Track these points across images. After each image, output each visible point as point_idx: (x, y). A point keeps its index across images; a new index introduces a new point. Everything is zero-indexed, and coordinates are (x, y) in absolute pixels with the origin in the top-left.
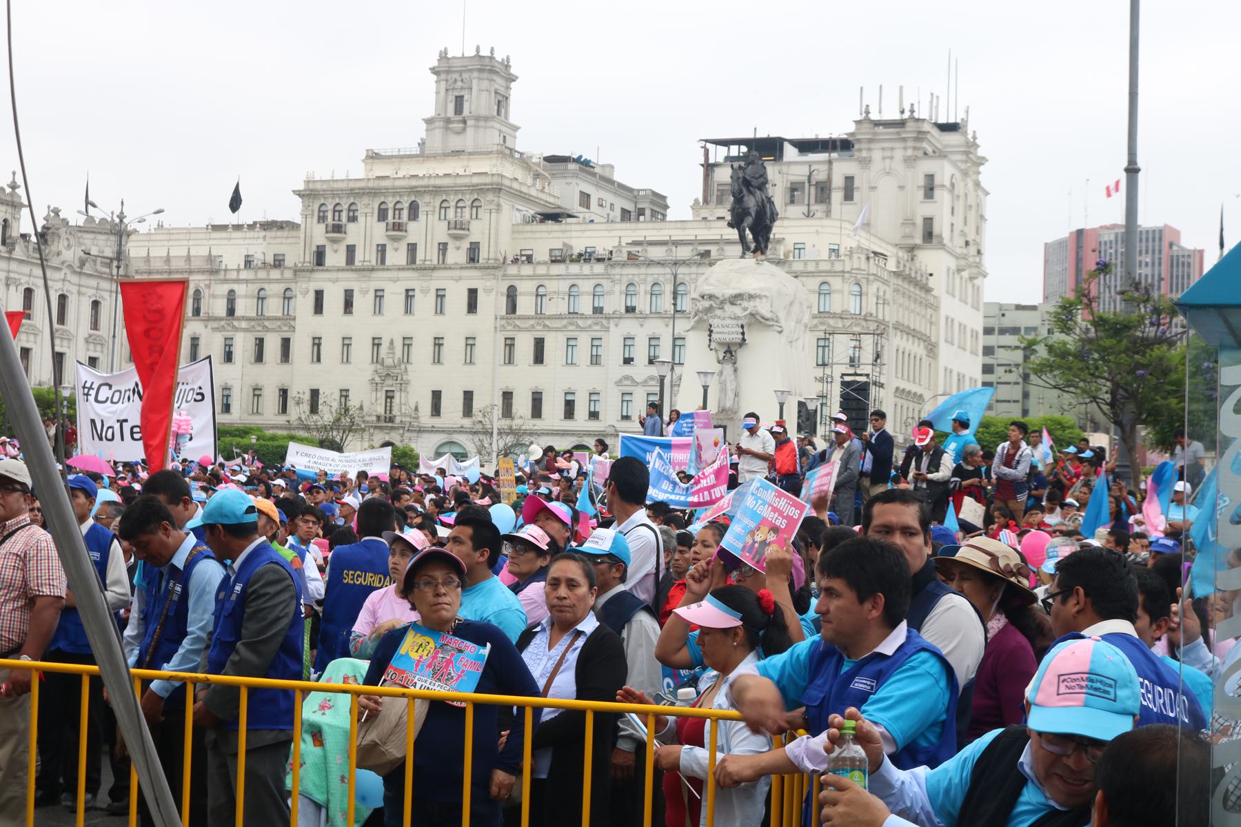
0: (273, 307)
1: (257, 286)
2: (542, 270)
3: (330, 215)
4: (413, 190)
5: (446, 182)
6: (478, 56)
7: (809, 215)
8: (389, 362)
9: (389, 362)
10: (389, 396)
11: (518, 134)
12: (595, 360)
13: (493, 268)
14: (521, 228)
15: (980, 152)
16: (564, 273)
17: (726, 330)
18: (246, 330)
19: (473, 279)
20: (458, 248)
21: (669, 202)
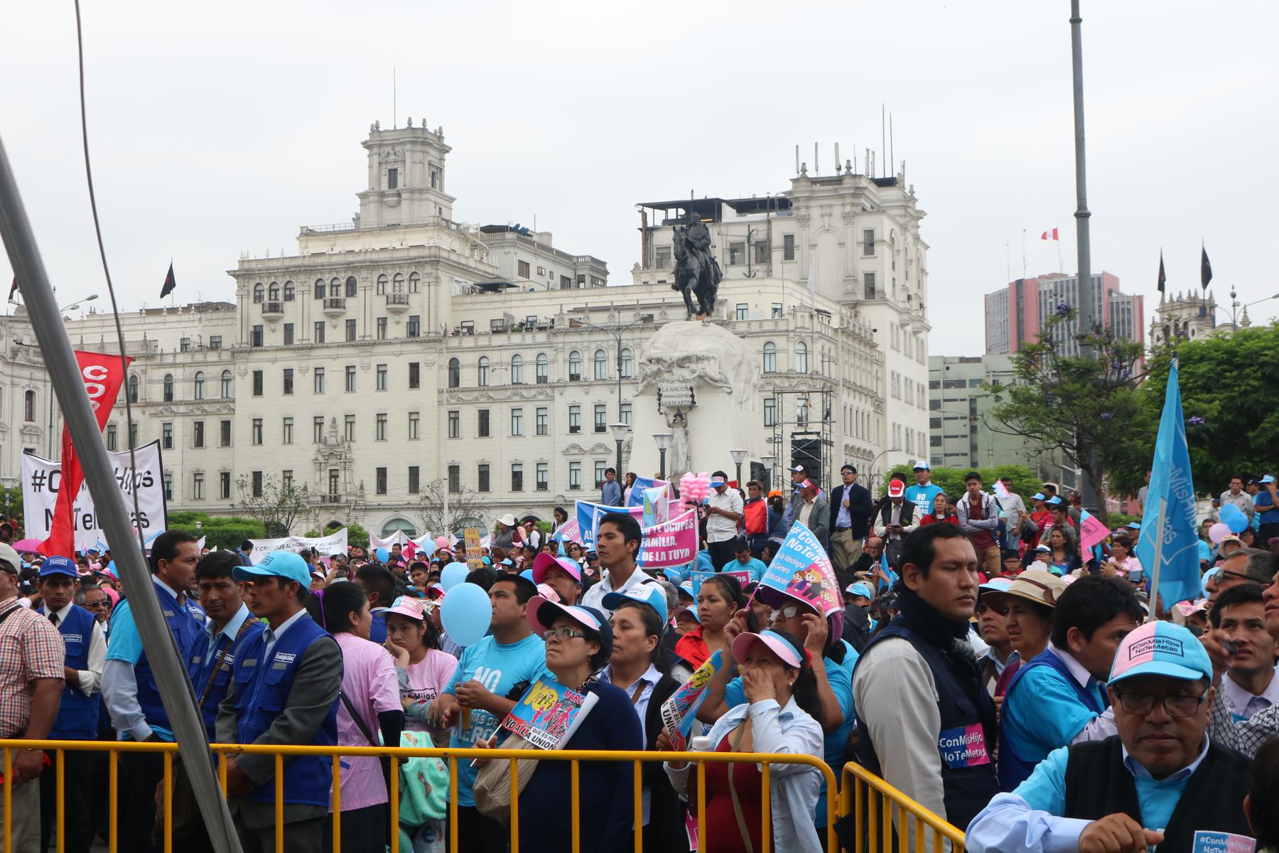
0: (212, 390)
1: (194, 370)
2: (483, 341)
3: (266, 294)
4: (350, 266)
5: (383, 256)
6: (410, 128)
7: (749, 276)
8: (332, 441)
9: (332, 441)
10: (334, 476)
11: (454, 205)
12: (541, 430)
13: (435, 341)
14: (460, 300)
15: (918, 206)
16: (506, 343)
17: (675, 393)
18: (184, 415)
19: (415, 353)
20: (398, 323)
21: (608, 267)
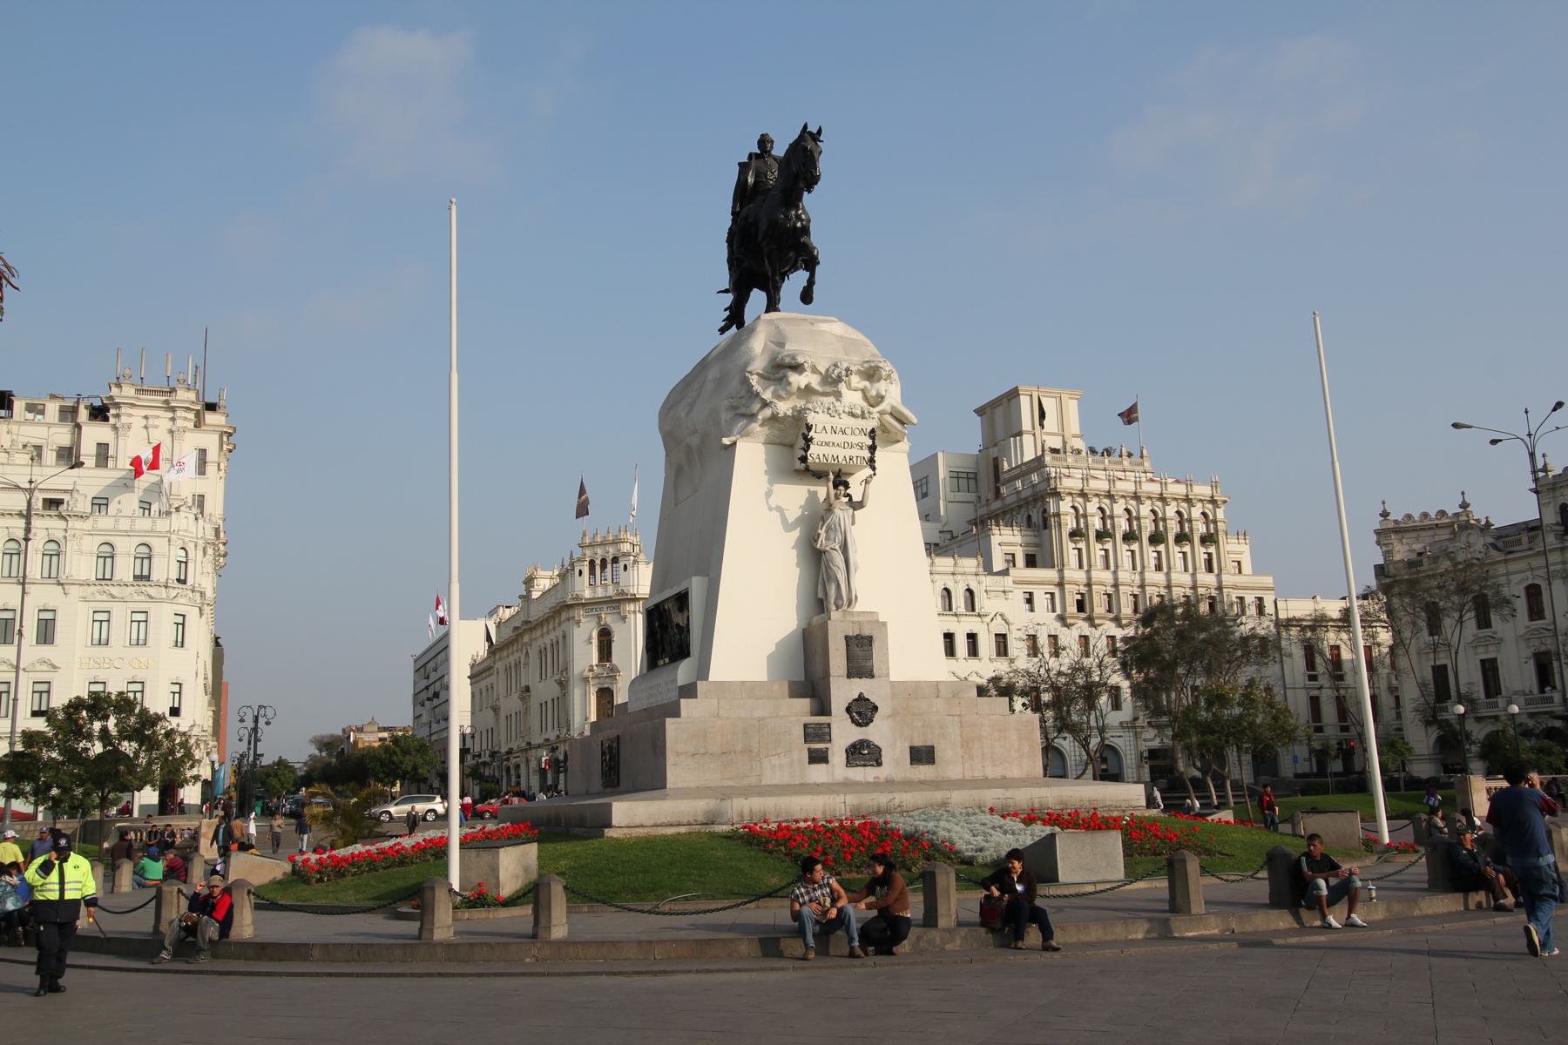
17: (839, 438)
